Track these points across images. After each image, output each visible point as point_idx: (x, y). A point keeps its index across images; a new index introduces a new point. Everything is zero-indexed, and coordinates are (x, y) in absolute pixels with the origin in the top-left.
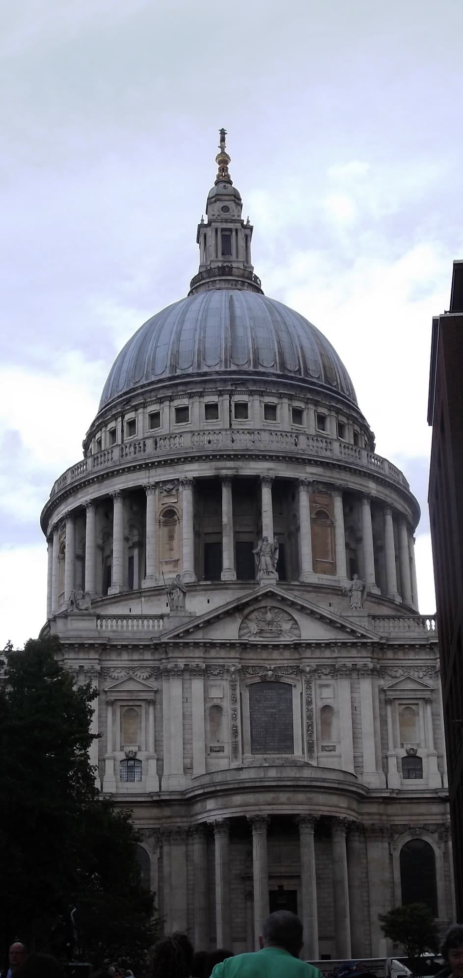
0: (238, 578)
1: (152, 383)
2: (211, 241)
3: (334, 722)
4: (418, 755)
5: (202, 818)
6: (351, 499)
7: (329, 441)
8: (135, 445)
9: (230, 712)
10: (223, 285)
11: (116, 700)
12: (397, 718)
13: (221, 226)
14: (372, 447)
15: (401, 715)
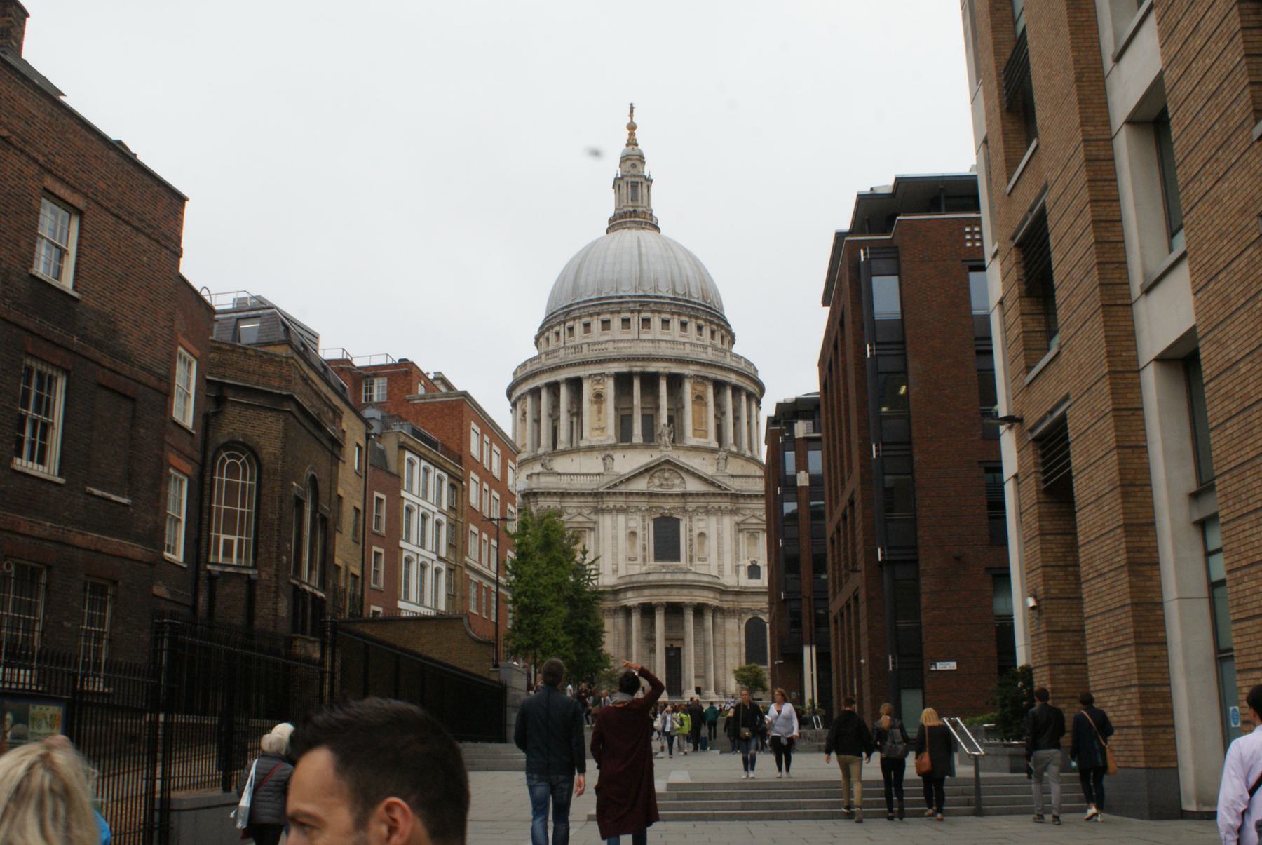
0: (644, 440)
1: (585, 302)
2: (624, 190)
3: (707, 543)
4: (758, 564)
5: (624, 603)
6: (719, 386)
7: (705, 347)
8: (574, 347)
9: (641, 536)
10: (632, 225)
11: (570, 527)
12: (746, 539)
13: (630, 180)
14: (733, 341)
15: (748, 539)
